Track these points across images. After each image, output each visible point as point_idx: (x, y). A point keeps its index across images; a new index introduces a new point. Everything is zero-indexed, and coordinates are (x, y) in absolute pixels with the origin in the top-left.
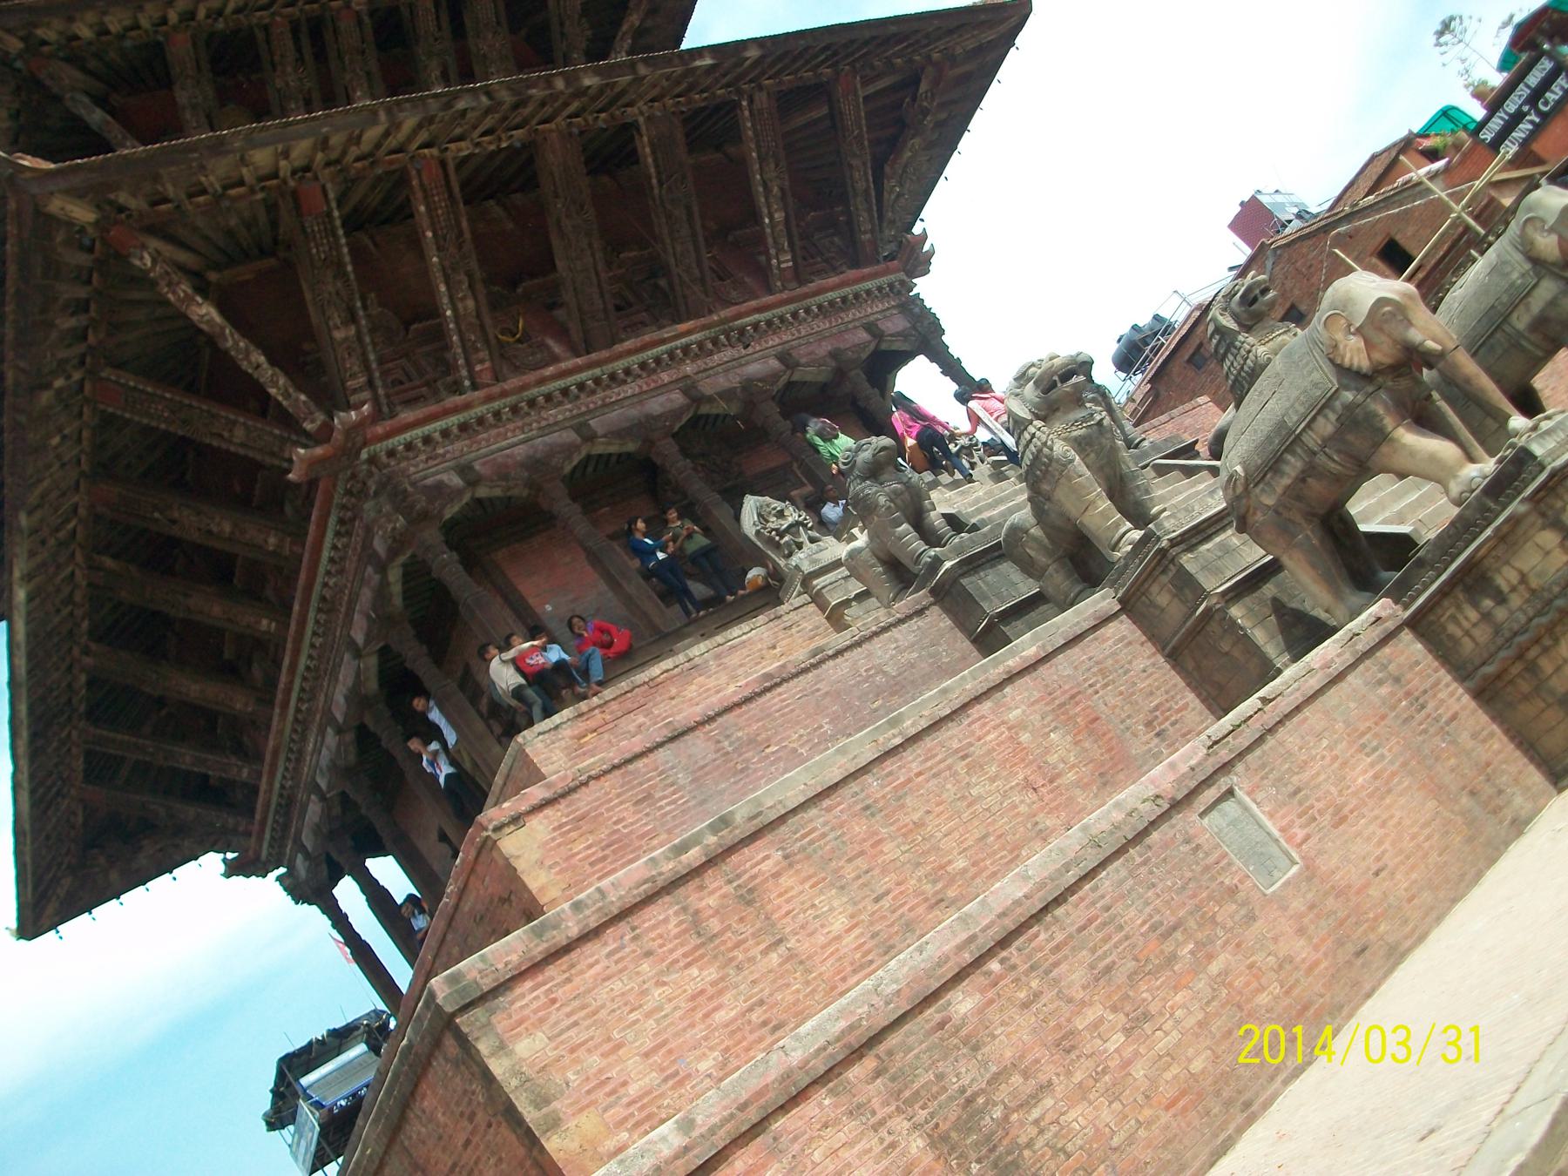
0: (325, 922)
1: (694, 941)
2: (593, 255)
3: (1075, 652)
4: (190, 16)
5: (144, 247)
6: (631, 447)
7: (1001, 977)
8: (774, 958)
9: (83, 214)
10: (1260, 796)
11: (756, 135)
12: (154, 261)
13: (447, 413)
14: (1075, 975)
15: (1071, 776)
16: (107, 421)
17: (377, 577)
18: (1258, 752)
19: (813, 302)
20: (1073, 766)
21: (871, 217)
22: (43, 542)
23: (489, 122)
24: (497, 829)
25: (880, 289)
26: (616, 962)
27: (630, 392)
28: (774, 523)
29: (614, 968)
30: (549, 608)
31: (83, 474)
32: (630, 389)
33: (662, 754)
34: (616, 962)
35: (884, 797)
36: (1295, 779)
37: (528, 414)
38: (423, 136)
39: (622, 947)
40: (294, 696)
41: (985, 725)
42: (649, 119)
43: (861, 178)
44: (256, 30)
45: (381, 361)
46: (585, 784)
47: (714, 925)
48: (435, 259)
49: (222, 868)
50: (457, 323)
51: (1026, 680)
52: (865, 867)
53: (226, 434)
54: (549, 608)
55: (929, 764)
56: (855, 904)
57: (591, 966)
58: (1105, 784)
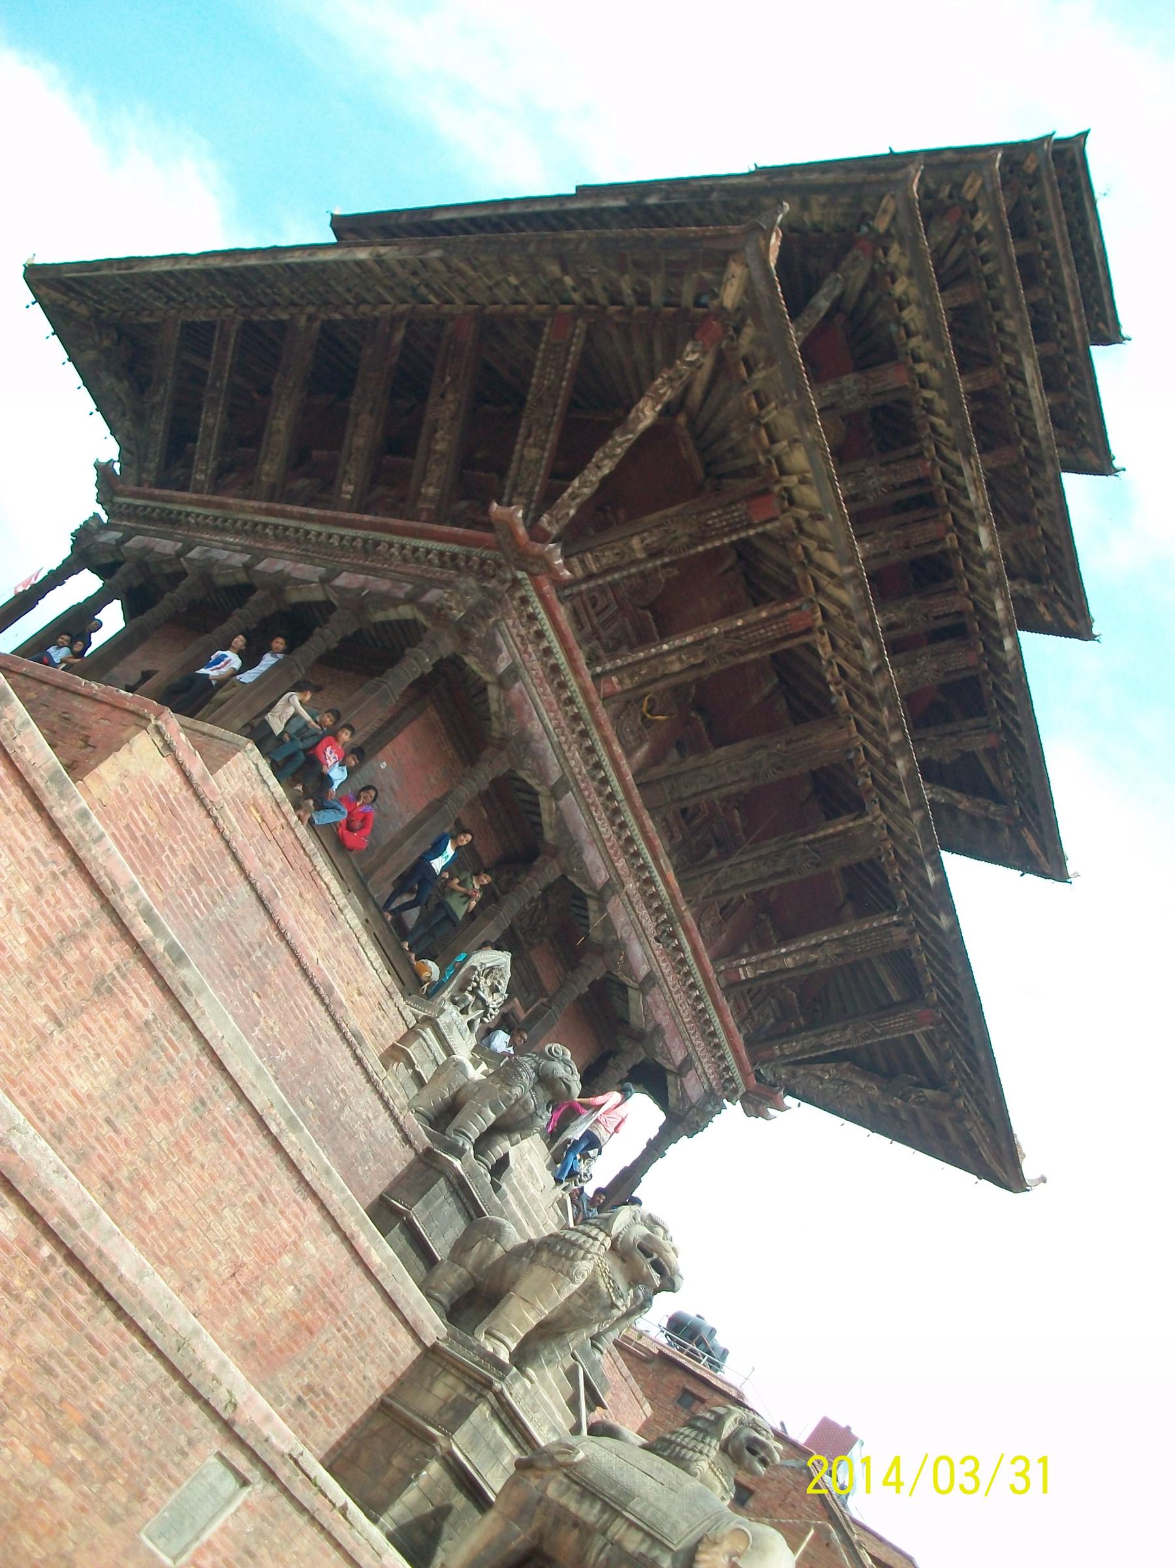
0: (55, 563)
1: (55, 936)
2: (734, 783)
3: (379, 1303)
4: (924, 383)
5: (704, 353)
6: (549, 835)
7: (34, 1257)
8: (42, 1019)
9: (730, 295)
10: (244, 1515)
11: (865, 932)
12: (691, 364)
13: (568, 652)
14: (42, 1336)
15: (249, 1311)
16: (535, 328)
17: (401, 595)
18: (289, 1508)
19: (708, 1002)
20: (260, 1313)
21: (796, 1054)
22: (415, 273)
23: (852, 672)
24: (158, 729)
25: (727, 1069)
26: (28, 858)
27: (602, 829)
28: (486, 984)
29: (22, 856)
30: (383, 765)
31: (484, 307)
32: (606, 830)
33: (244, 889)
34: (28, 858)
35: (215, 1119)
36: (264, 1551)
37: (573, 732)
38: (833, 610)
39: (45, 864)
40: (280, 521)
41: (297, 1217)
42: (871, 827)
43: (835, 1039)
44: (917, 446)
45: (614, 585)
46: (209, 815)
47: (73, 956)
48: (716, 630)
49: (104, 459)
50: (655, 656)
51: (346, 1256)
52: (142, 1106)
53: (531, 441)
54: (383, 765)
55: (252, 1163)
56: (103, 1098)
57: (23, 833)
58: (244, 1348)
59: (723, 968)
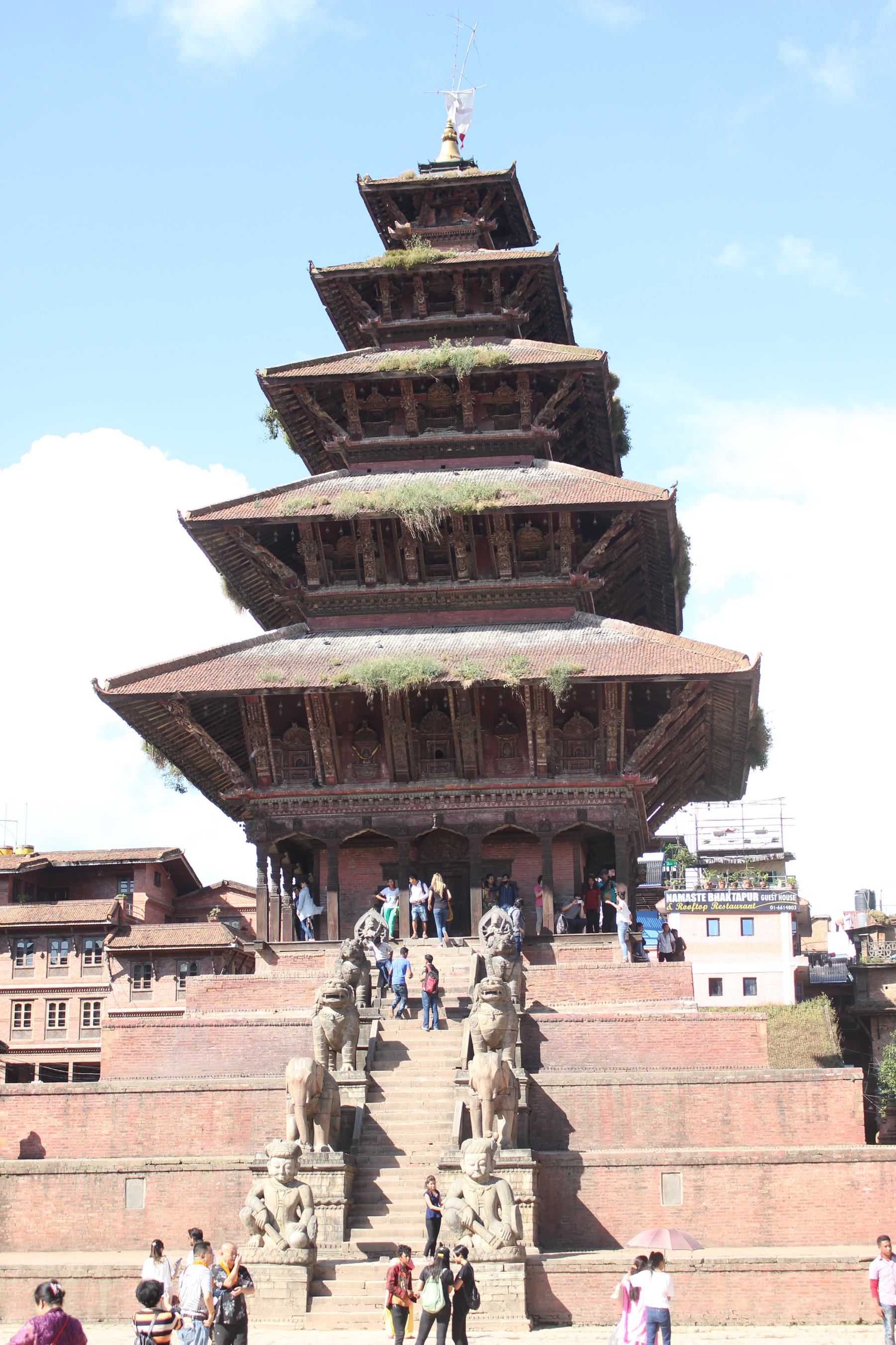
12: (173, 710)
13: (298, 795)
15: (219, 1133)
21: (618, 751)
25: (600, 793)
47: (71, 1111)
59: (532, 773)
